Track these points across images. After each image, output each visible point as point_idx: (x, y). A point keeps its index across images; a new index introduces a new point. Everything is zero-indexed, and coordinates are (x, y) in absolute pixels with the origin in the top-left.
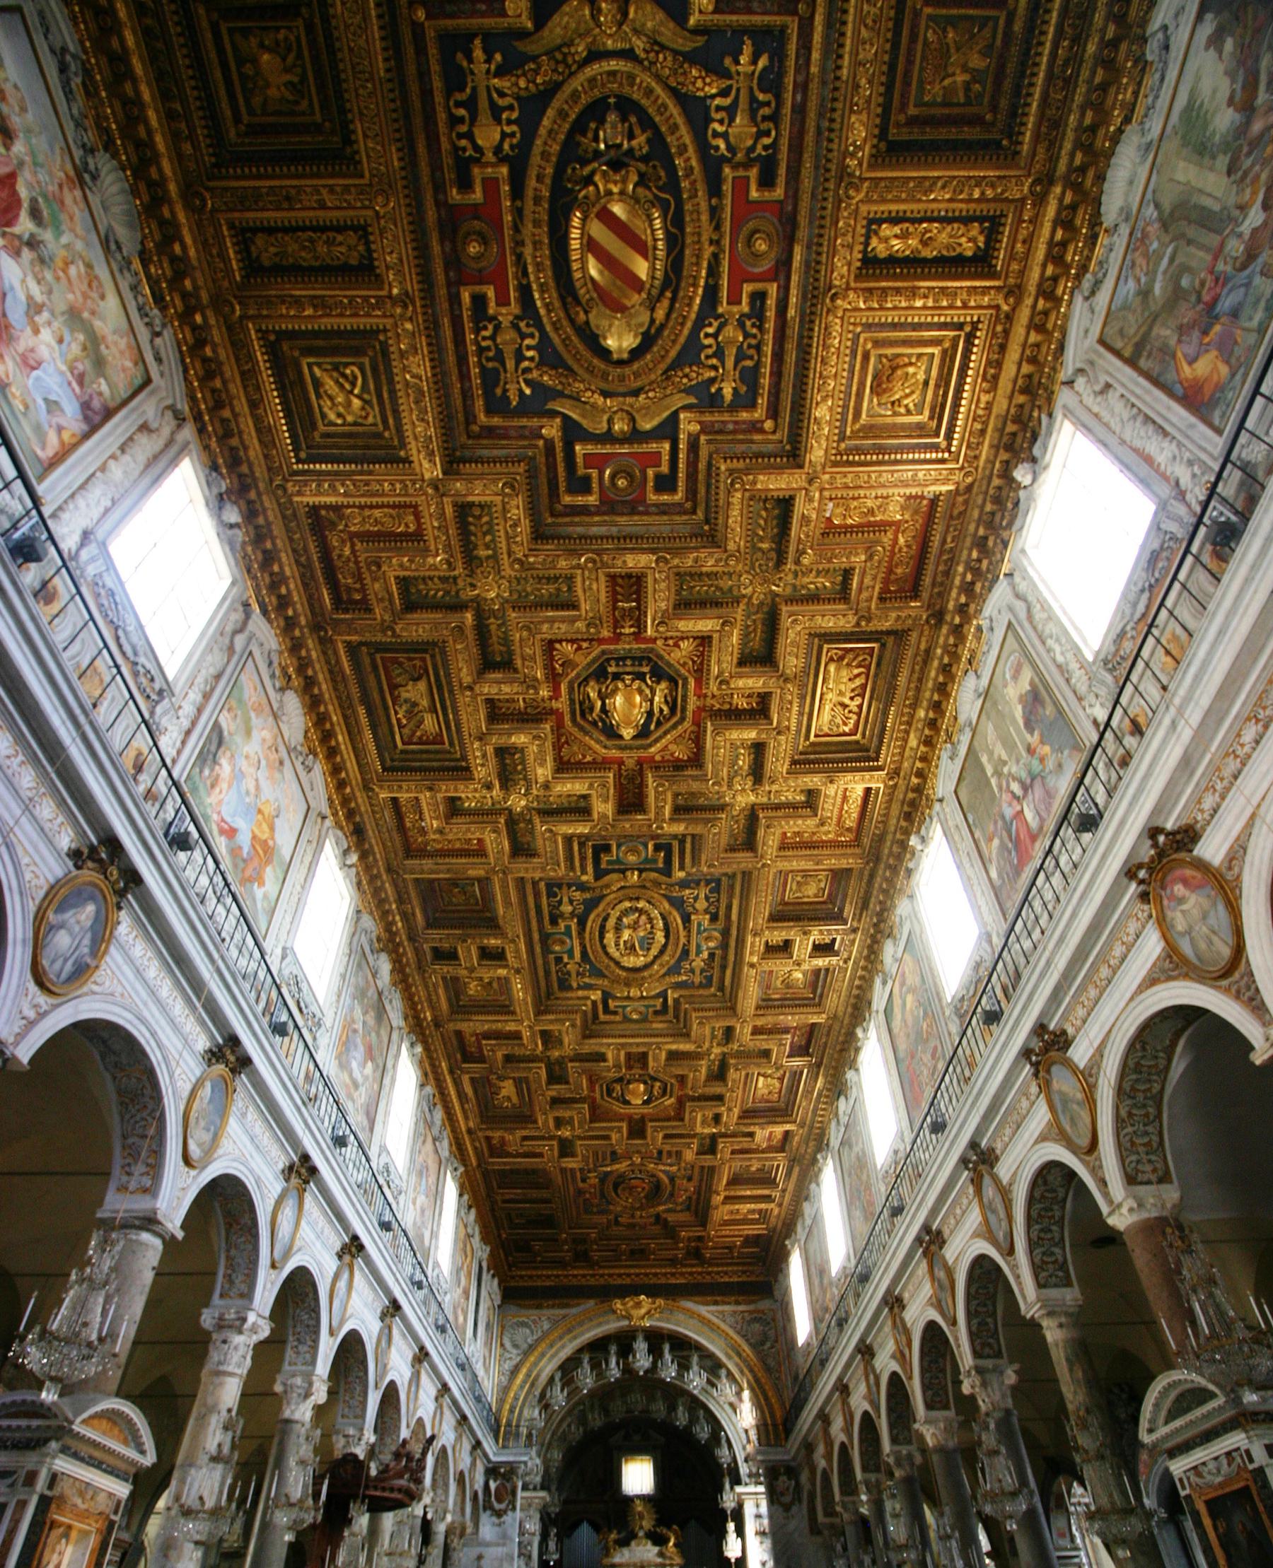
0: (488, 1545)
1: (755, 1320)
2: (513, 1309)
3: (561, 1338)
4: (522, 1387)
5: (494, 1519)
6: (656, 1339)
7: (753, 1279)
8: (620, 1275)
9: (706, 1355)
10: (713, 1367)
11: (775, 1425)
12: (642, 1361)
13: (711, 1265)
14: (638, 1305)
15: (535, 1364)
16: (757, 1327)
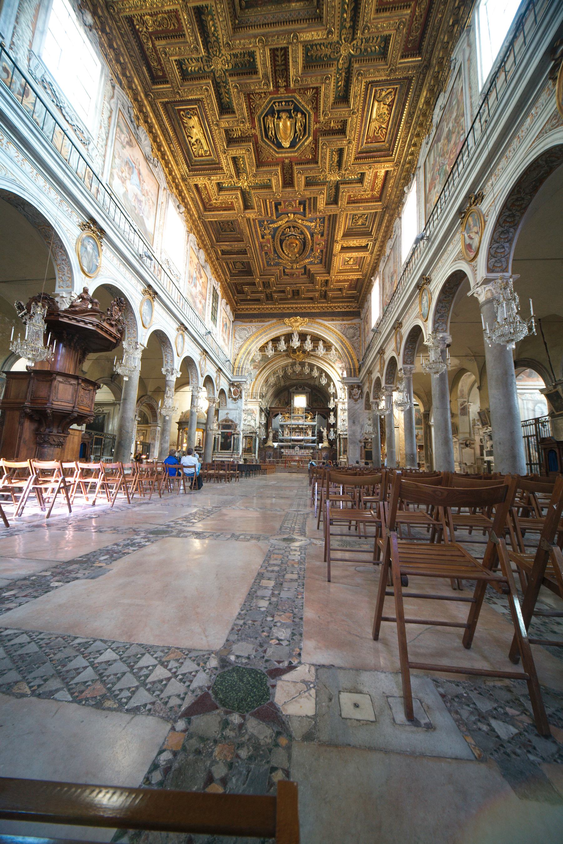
0: (231, 410)
1: (351, 328)
2: (239, 323)
3: (261, 335)
4: (244, 354)
6: (303, 337)
7: (351, 310)
8: (288, 308)
9: (325, 342)
10: (328, 347)
11: (355, 369)
12: (296, 343)
13: (332, 302)
14: (296, 321)
15: (250, 345)
16: (351, 331)
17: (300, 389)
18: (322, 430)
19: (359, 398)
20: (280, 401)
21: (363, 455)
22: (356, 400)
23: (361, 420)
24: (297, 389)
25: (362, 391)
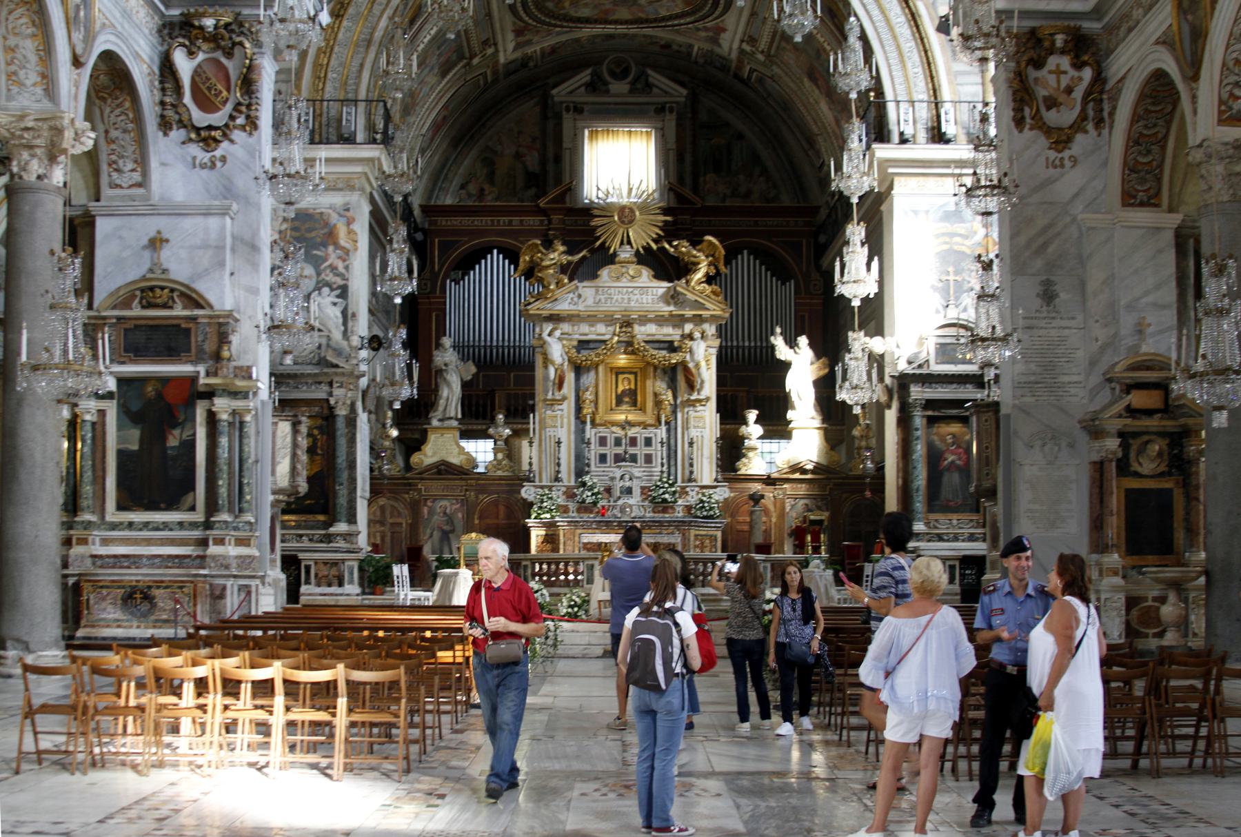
0: (179, 212)
5: (195, 150)
17: (619, 87)
18: (782, 351)
19: (1078, 126)
20: (489, 161)
21: (1114, 526)
22: (1061, 139)
23: (1095, 277)
24: (595, 86)
25: (1099, 78)
